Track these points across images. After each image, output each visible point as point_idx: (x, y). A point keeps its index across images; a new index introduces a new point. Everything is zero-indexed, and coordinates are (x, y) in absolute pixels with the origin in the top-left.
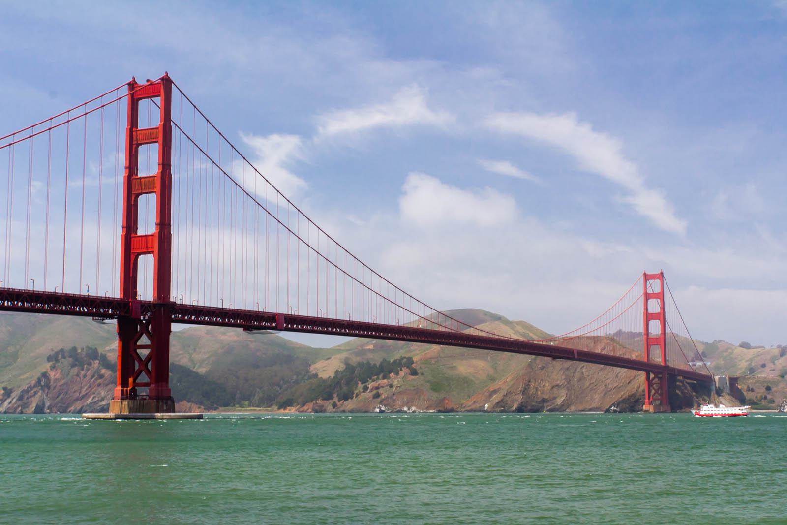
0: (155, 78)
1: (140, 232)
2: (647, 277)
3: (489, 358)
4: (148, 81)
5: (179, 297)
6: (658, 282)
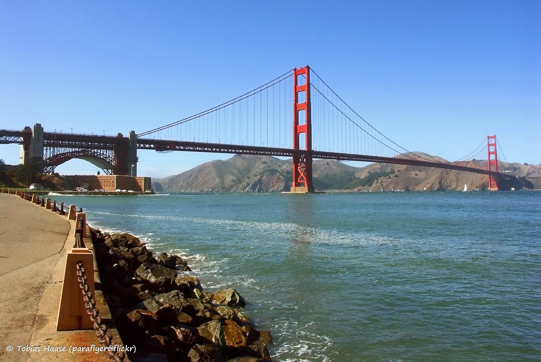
0: (304, 66)
2: (489, 137)
6: (494, 139)
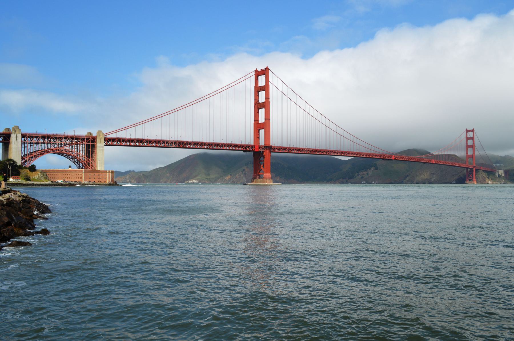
0: (263, 68)
1: (260, 122)
3: (407, 163)
4: (261, 69)
5: (274, 144)
6: (472, 133)
